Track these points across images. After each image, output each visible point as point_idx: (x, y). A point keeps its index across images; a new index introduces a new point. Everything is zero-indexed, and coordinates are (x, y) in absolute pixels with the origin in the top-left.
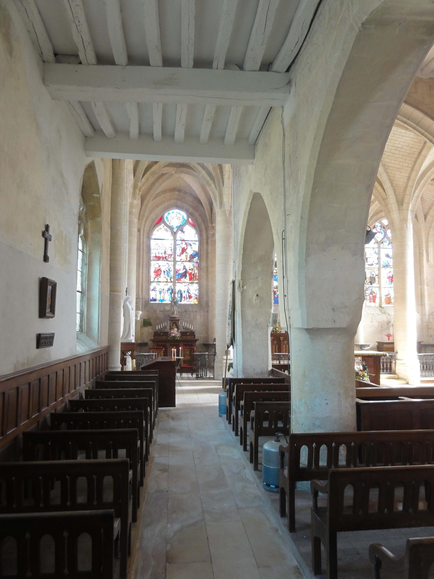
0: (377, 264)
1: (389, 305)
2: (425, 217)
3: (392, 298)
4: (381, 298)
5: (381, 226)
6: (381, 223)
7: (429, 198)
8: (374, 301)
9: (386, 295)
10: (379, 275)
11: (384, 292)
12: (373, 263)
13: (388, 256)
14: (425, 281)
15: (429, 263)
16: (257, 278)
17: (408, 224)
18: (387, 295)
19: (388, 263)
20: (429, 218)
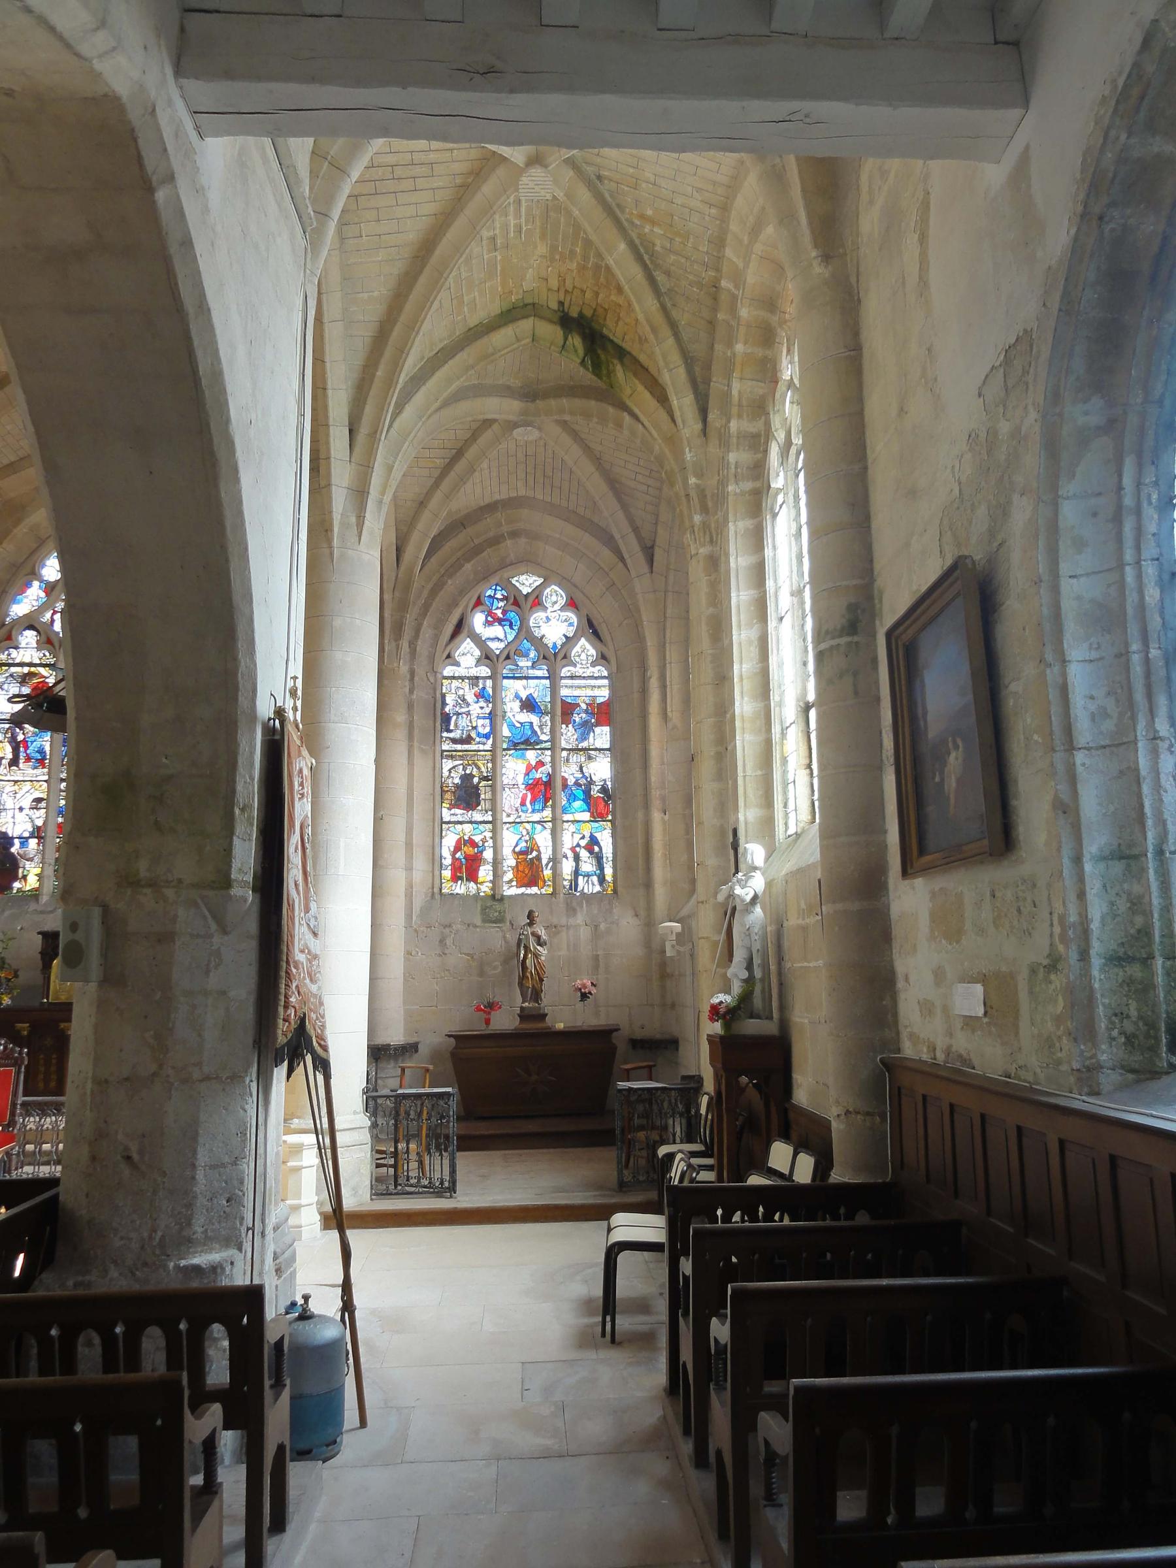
0: (487, 736)
1: (534, 890)
2: (649, 553)
3: (544, 862)
4: (497, 863)
5: (505, 598)
6: (507, 585)
7: (639, 477)
8: (473, 876)
9: (521, 853)
10: (491, 778)
11: (510, 839)
12: (473, 735)
13: (529, 705)
14: (655, 794)
15: (670, 725)
17: (336, 542)
18: (525, 853)
20: (659, 555)
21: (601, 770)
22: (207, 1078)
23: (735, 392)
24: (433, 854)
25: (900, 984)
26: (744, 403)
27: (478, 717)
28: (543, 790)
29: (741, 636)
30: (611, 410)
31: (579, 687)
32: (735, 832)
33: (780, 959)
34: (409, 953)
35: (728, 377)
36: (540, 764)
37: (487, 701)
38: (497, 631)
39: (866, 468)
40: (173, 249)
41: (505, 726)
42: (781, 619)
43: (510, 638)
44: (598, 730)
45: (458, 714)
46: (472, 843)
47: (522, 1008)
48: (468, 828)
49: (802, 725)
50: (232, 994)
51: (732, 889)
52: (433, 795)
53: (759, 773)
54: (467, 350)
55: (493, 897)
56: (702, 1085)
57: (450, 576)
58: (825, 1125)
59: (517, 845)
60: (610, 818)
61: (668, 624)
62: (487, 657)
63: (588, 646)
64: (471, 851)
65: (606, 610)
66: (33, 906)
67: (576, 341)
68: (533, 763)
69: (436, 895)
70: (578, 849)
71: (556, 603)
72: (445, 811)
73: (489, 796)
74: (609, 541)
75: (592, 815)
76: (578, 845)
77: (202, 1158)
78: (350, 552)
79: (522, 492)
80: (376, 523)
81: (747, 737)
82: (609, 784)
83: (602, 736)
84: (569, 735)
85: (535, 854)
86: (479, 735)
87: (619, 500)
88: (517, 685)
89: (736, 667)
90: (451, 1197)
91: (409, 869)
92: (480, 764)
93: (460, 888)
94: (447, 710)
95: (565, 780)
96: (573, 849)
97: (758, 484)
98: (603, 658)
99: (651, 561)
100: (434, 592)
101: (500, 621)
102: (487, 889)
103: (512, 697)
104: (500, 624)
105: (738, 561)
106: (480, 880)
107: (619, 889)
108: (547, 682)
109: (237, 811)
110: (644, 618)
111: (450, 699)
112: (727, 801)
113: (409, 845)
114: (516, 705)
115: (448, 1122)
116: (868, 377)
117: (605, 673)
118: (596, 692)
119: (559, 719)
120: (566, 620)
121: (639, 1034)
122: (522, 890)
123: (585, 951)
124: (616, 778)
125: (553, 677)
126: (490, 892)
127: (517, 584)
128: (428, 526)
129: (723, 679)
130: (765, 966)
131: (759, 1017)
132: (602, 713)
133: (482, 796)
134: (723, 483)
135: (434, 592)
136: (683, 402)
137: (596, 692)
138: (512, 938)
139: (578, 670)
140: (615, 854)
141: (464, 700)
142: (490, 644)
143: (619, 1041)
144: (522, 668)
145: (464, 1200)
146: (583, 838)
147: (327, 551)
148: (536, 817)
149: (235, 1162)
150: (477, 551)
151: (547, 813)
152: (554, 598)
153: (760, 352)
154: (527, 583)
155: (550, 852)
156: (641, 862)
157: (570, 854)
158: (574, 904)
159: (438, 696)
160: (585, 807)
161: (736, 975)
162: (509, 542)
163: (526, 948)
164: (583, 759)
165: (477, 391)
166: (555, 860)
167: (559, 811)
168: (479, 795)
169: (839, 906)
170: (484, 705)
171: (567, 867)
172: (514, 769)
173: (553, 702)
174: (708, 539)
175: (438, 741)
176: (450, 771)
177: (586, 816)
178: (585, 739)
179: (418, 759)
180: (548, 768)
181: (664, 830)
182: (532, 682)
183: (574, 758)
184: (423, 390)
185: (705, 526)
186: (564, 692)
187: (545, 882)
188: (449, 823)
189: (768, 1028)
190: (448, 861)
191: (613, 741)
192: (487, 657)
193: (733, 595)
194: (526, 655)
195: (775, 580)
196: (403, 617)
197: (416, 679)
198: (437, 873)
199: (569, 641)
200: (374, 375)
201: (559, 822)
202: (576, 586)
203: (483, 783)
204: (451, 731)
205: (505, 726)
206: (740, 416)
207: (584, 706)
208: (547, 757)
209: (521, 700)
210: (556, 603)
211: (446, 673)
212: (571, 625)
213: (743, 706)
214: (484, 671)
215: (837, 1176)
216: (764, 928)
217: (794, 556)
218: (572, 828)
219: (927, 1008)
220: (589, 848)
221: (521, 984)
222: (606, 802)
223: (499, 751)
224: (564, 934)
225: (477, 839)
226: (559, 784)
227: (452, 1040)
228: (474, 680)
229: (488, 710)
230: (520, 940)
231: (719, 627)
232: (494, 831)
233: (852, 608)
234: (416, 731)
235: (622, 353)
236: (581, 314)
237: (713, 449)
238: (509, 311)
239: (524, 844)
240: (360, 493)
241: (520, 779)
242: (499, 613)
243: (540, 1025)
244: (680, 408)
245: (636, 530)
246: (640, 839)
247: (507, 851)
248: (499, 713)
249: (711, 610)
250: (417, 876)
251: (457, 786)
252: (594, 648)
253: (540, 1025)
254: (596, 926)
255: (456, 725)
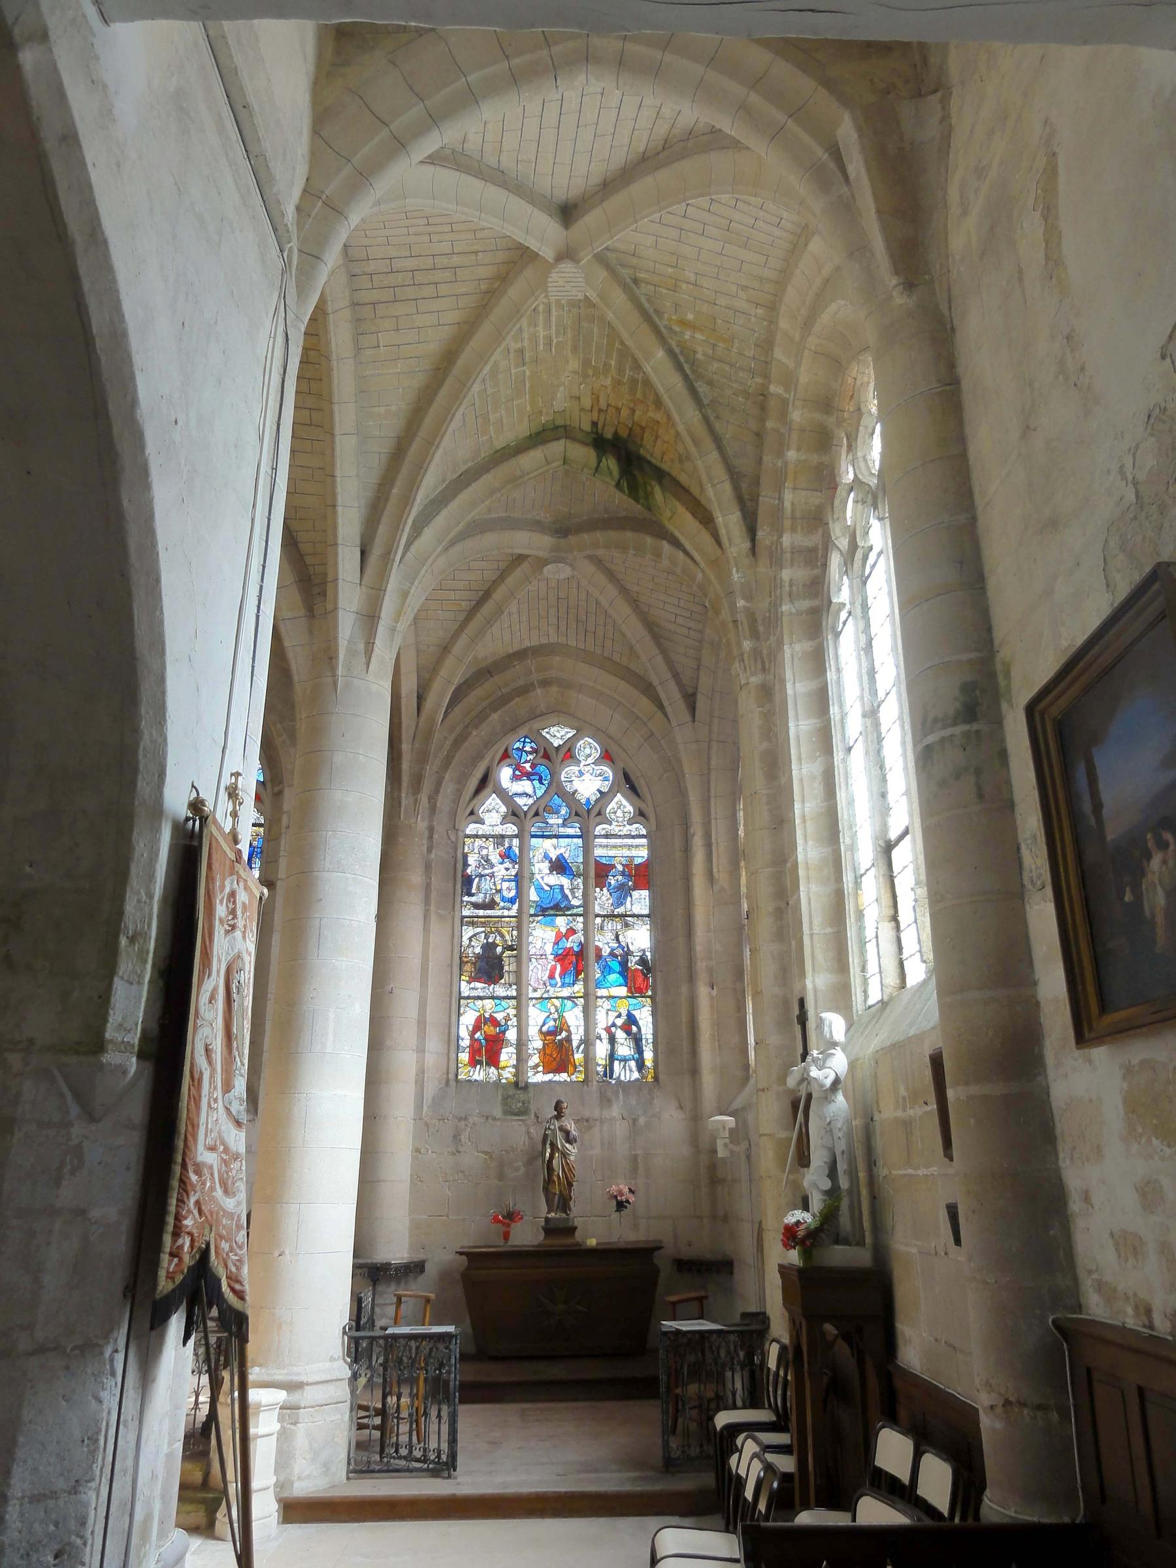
0: (512, 901)
1: (563, 1077)
2: (691, 701)
3: (575, 1044)
4: (521, 1045)
5: (535, 751)
6: (536, 737)
7: (680, 620)
8: (493, 1060)
9: (549, 1033)
11: (536, 1017)
12: (497, 899)
13: (559, 866)
14: (701, 965)
15: (716, 888)
17: (340, 671)
18: (553, 1033)
19: (565, 897)
20: (701, 702)
21: (640, 939)
22: (41, 1350)
23: (787, 504)
24: (449, 1033)
25: (1075, 1205)
26: (798, 514)
27: (503, 880)
28: (574, 962)
29: (803, 771)
30: (649, 540)
31: (615, 847)
32: (802, 1003)
33: (871, 1163)
34: (418, 1151)
35: (779, 488)
36: (572, 931)
37: (513, 862)
38: (525, 786)
39: (974, 519)
40: (50, 145)
41: (532, 889)
42: (849, 749)
43: (539, 793)
44: (636, 894)
45: (481, 876)
46: (494, 1022)
47: (547, 1219)
48: (489, 1003)
49: (883, 869)
50: (95, 1214)
51: (806, 1071)
52: (451, 966)
53: (829, 930)
54: (493, 472)
55: (516, 1084)
56: (768, 1327)
57: (476, 727)
58: (969, 1415)
59: (544, 1024)
60: (650, 993)
61: (713, 778)
62: (514, 814)
63: (625, 802)
64: (490, 1030)
65: (644, 764)
67: (611, 463)
68: (563, 930)
69: (452, 1082)
70: (613, 1029)
71: (589, 756)
72: (463, 984)
73: (513, 967)
74: (649, 690)
75: (629, 990)
76: (613, 1025)
77: (20, 1484)
78: (356, 681)
79: (554, 639)
80: (384, 653)
81: (814, 888)
82: (648, 954)
83: (640, 901)
84: (603, 900)
85: (564, 1034)
86: (503, 899)
87: (659, 645)
88: (548, 844)
89: (797, 806)
90: (449, 1477)
91: (421, 1050)
92: (504, 931)
93: (478, 1074)
94: (469, 871)
95: (598, 950)
96: (608, 1029)
97: (816, 602)
98: (641, 815)
99: (692, 708)
100: (458, 743)
101: (528, 776)
102: (509, 1076)
103: (541, 857)
104: (529, 779)
105: (796, 688)
106: (502, 1064)
107: (661, 1077)
108: (580, 841)
109: (123, 941)
110: (686, 770)
111: (472, 860)
112: (790, 965)
113: (422, 1024)
114: (547, 864)
115: (449, 1372)
116: (972, 409)
117: (644, 832)
118: (634, 853)
119: (592, 881)
120: (600, 775)
121: (686, 1253)
122: (549, 1077)
123: (622, 1149)
124: (655, 949)
125: (586, 836)
126: (513, 1079)
127: (548, 736)
128: (452, 673)
129: (781, 821)
130: (852, 1173)
131: (846, 1242)
132: (640, 876)
133: (506, 968)
134: (775, 605)
135: (458, 743)
136: (729, 521)
137: (634, 853)
138: (537, 1133)
139: (614, 828)
140: (655, 1035)
141: (487, 860)
142: (517, 799)
143: (662, 1261)
144: (552, 826)
145: (469, 1481)
146: (619, 1016)
147: (329, 680)
148: (566, 992)
149: (75, 1488)
150: (504, 701)
151: (579, 988)
152: (588, 751)
153: (814, 458)
154: (559, 735)
155: (581, 1030)
156: (685, 1044)
157: (604, 1035)
158: (609, 1094)
159: (460, 856)
160: (621, 980)
161: (816, 1186)
162: (539, 691)
163: (553, 1146)
164: (619, 927)
165: (508, 524)
166: (588, 1042)
167: (592, 985)
168: (502, 967)
169: (975, 1089)
170: (510, 866)
171: (601, 1050)
172: (542, 938)
173: (585, 863)
174: (759, 666)
175: (458, 906)
176: (470, 939)
177: (623, 991)
178: (622, 904)
179: (434, 925)
180: (580, 936)
181: (712, 1007)
182: (563, 842)
183: (609, 925)
184: (445, 513)
185: (756, 653)
186: (598, 852)
187: (575, 1067)
188: (468, 998)
189: (861, 1257)
190: (466, 1043)
191: (653, 907)
192: (513, 814)
193: (791, 724)
194: (557, 812)
195: (841, 706)
196: (422, 769)
197: (435, 836)
198: (453, 1056)
199: (604, 796)
200: (389, 492)
201: (592, 998)
202: (610, 737)
203: (508, 953)
204: (473, 895)
205: (532, 889)
206: (793, 530)
207: (620, 868)
208: (579, 924)
209: (551, 861)
210: (589, 756)
211: (468, 832)
212: (606, 779)
213: (808, 851)
214: (511, 829)
215: (999, 1506)
216: (848, 1122)
217: (864, 671)
218: (607, 1005)
219: (1129, 1245)
220: (626, 1028)
221: (546, 1190)
222: (645, 976)
223: (525, 917)
224: (596, 1130)
225: (499, 1016)
226: (592, 955)
227: (464, 1257)
228: (500, 839)
229: (513, 872)
230: (545, 1136)
231: (776, 763)
232: (518, 1008)
233: (968, 688)
234: (434, 895)
235: (661, 475)
236: (616, 434)
237: (763, 568)
238: (538, 434)
239: (552, 1023)
240: (370, 618)
241: (549, 949)
242: (528, 766)
243: (569, 1241)
244: (726, 526)
245: (676, 675)
246: (685, 1017)
247: (533, 1031)
248: (526, 875)
249: (765, 745)
250: (430, 1059)
251: (478, 956)
252: (632, 804)
253: (569, 1241)
254: (635, 1121)
255: (478, 887)
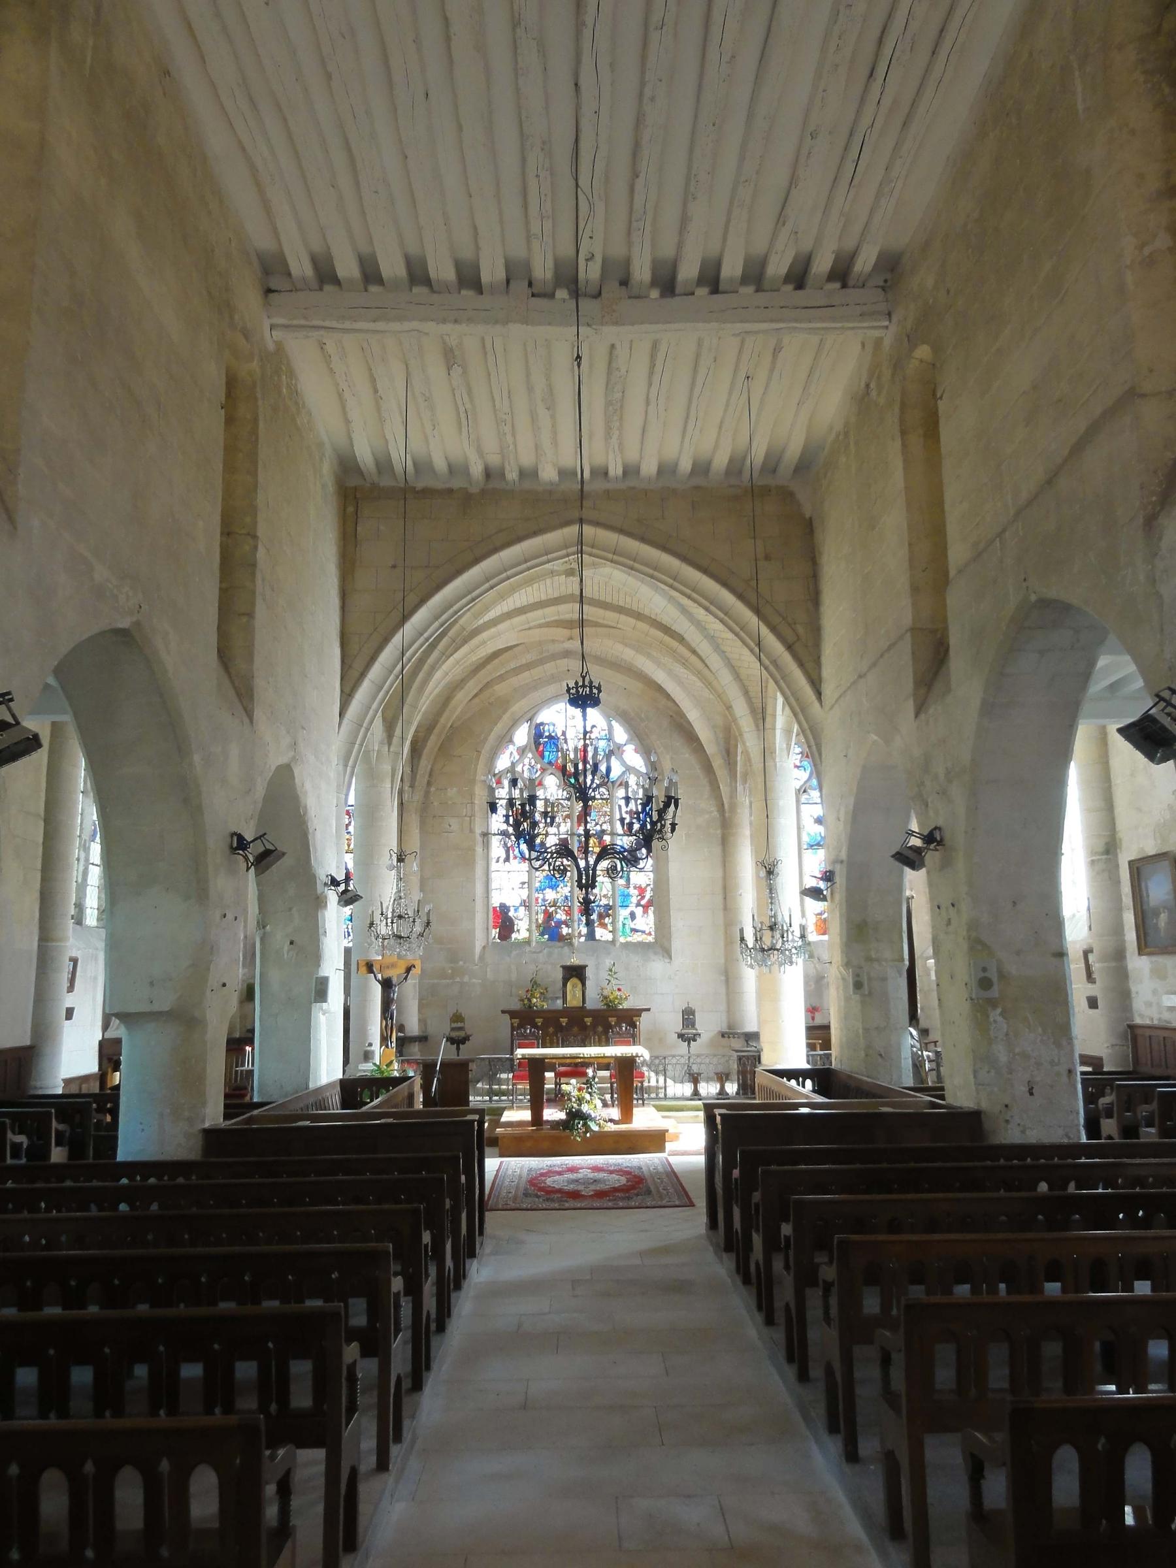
16: (290, 909)
18: (821, 914)
25: (1133, 995)
66: (528, 949)
219: (1149, 1004)
233: (1107, 844)
